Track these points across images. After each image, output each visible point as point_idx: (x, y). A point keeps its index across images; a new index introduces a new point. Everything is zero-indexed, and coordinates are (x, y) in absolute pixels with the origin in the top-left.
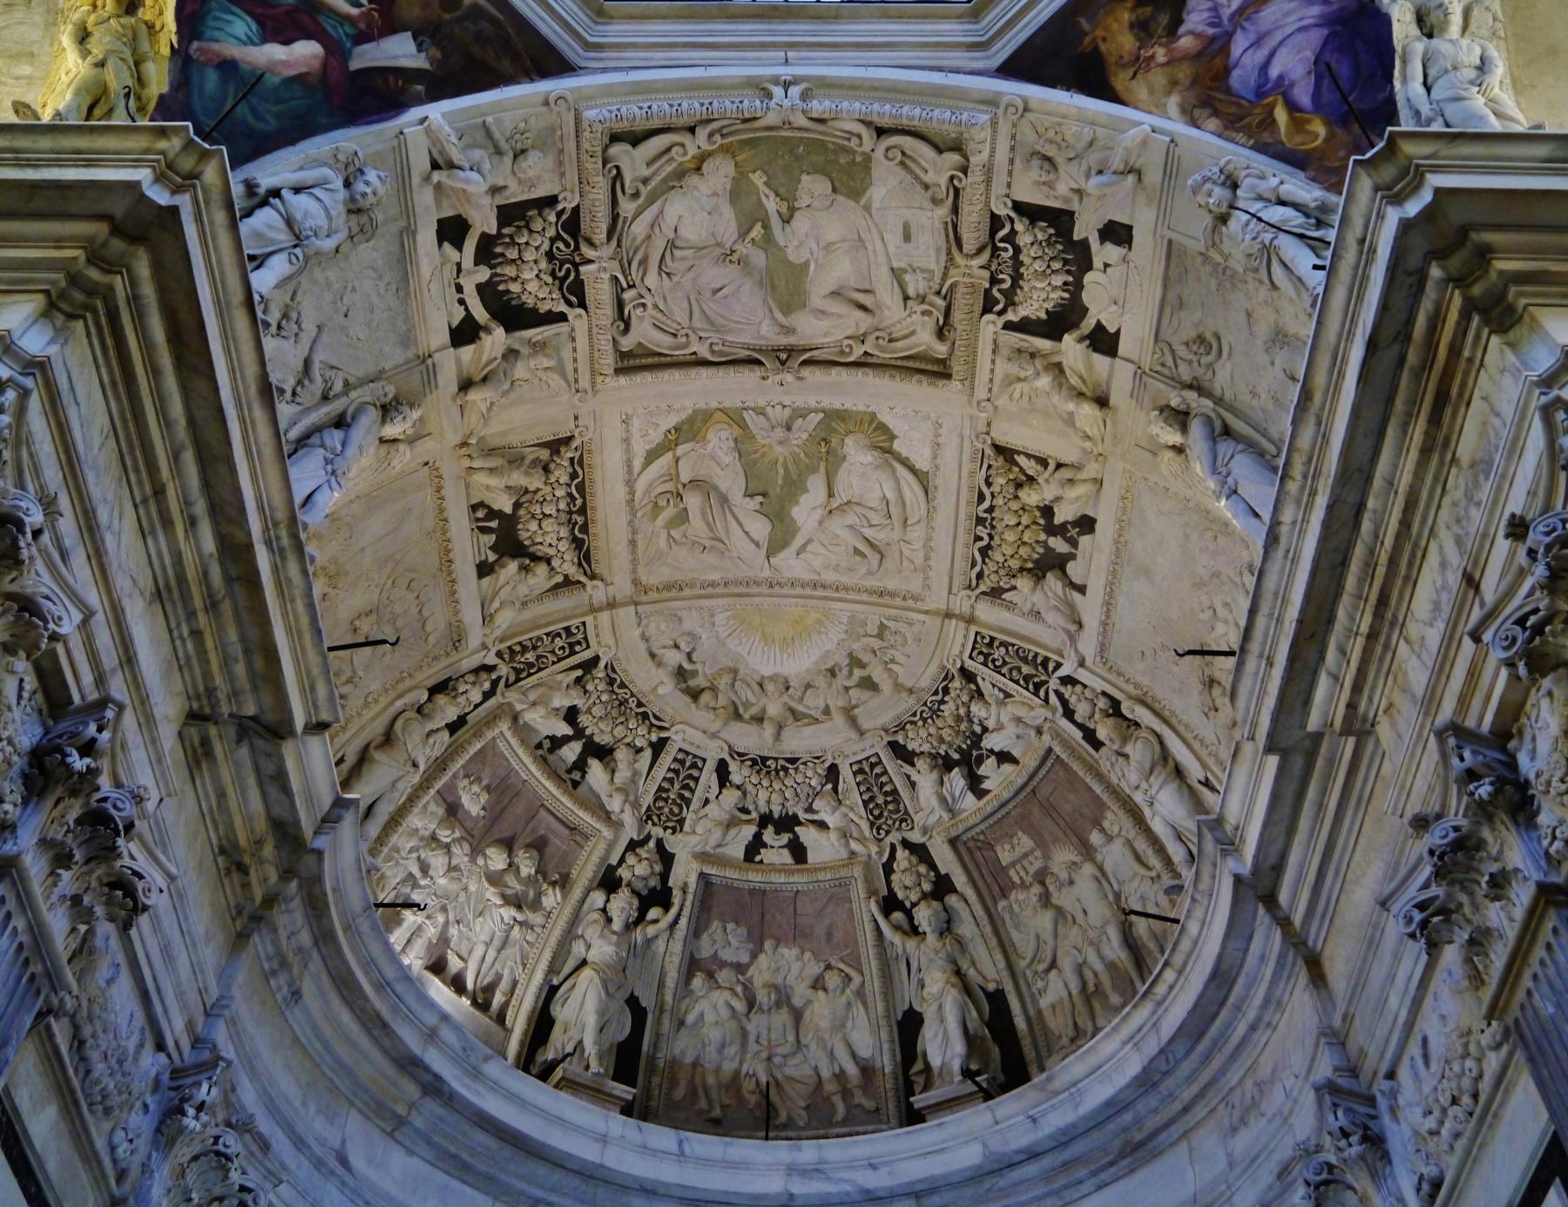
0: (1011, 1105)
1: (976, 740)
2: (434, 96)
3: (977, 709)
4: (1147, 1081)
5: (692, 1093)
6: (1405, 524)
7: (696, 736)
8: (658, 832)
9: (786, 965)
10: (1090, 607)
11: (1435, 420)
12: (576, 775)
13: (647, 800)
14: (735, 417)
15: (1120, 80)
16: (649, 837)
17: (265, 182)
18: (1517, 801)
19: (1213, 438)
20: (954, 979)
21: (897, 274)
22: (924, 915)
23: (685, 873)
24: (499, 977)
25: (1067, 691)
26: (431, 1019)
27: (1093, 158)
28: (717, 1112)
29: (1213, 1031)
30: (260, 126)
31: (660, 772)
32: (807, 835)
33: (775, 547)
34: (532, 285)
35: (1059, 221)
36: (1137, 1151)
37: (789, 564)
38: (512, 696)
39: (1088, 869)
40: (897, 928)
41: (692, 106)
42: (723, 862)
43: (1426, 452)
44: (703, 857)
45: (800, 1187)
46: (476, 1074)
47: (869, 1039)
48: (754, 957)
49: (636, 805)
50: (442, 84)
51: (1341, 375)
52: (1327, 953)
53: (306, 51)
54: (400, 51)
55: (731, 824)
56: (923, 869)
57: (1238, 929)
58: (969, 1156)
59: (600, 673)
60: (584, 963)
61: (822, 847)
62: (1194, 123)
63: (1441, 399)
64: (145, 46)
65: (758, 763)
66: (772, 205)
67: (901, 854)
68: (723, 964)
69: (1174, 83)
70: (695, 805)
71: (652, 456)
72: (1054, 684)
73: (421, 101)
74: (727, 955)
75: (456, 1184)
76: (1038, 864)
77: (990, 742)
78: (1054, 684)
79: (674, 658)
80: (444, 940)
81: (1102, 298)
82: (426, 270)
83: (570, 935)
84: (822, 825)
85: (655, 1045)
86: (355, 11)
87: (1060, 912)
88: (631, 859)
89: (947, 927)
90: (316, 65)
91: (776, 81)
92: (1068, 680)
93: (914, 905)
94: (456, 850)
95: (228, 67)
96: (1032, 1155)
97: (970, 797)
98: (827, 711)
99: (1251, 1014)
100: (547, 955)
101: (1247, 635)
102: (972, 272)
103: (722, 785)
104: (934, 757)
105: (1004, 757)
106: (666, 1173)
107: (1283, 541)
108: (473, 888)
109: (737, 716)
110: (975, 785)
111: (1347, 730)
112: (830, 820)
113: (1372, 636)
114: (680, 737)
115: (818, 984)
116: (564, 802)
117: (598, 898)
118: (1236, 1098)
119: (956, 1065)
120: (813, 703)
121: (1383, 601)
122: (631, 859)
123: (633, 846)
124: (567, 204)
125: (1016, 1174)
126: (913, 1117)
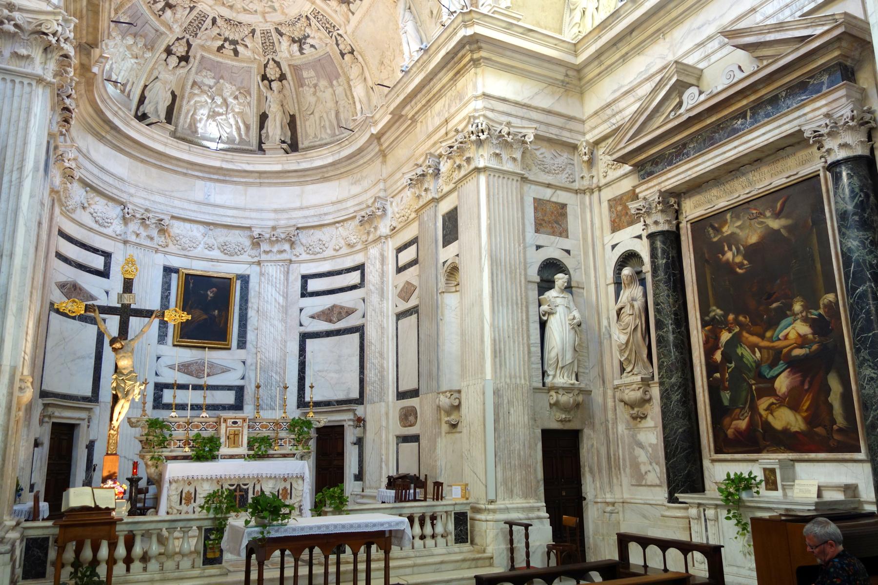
0: (293, 156)
1: (306, 37)
3: (308, 30)
4: (332, 164)
6: (440, 90)
7: (208, 8)
8: (187, 36)
10: (354, 20)
11: (456, 75)
12: (161, 13)
13: (186, 25)
16: (183, 38)
18: (437, 173)
20: (281, 108)
22: (275, 85)
23: (196, 53)
24: (128, 81)
25: (339, 38)
26: (116, 109)
29: (354, 159)
32: (240, 49)
39: (330, 90)
40: (265, 86)
43: (451, 80)
44: (202, 47)
46: (128, 124)
49: (181, 26)
51: (439, 52)
52: (389, 156)
55: (213, 39)
56: (278, 69)
57: (369, 142)
58: (278, 168)
60: (157, 78)
63: (458, 72)
65: (228, 21)
67: (271, 62)
68: (205, 85)
70: (203, 29)
72: (335, 34)
75: (118, 154)
76: (315, 82)
77: (308, 40)
78: (335, 34)
80: (111, 69)
83: (153, 69)
84: (246, 46)
87: (318, 97)
88: (177, 44)
92: (339, 35)
93: (273, 81)
94: (117, 39)
96: (296, 171)
97: (298, 53)
98: (256, 11)
99: (365, 160)
100: (145, 76)
101: (395, 86)
103: (213, 24)
104: (290, 37)
105: (312, 46)
107: (411, 74)
108: (121, 50)
110: (301, 50)
111: (411, 119)
112: (249, 45)
113: (424, 106)
116: (156, 23)
117: (164, 56)
118: (355, 176)
119: (278, 138)
121: (429, 101)
122: (177, 44)
123: (178, 39)
125: (290, 174)
126: (261, 149)
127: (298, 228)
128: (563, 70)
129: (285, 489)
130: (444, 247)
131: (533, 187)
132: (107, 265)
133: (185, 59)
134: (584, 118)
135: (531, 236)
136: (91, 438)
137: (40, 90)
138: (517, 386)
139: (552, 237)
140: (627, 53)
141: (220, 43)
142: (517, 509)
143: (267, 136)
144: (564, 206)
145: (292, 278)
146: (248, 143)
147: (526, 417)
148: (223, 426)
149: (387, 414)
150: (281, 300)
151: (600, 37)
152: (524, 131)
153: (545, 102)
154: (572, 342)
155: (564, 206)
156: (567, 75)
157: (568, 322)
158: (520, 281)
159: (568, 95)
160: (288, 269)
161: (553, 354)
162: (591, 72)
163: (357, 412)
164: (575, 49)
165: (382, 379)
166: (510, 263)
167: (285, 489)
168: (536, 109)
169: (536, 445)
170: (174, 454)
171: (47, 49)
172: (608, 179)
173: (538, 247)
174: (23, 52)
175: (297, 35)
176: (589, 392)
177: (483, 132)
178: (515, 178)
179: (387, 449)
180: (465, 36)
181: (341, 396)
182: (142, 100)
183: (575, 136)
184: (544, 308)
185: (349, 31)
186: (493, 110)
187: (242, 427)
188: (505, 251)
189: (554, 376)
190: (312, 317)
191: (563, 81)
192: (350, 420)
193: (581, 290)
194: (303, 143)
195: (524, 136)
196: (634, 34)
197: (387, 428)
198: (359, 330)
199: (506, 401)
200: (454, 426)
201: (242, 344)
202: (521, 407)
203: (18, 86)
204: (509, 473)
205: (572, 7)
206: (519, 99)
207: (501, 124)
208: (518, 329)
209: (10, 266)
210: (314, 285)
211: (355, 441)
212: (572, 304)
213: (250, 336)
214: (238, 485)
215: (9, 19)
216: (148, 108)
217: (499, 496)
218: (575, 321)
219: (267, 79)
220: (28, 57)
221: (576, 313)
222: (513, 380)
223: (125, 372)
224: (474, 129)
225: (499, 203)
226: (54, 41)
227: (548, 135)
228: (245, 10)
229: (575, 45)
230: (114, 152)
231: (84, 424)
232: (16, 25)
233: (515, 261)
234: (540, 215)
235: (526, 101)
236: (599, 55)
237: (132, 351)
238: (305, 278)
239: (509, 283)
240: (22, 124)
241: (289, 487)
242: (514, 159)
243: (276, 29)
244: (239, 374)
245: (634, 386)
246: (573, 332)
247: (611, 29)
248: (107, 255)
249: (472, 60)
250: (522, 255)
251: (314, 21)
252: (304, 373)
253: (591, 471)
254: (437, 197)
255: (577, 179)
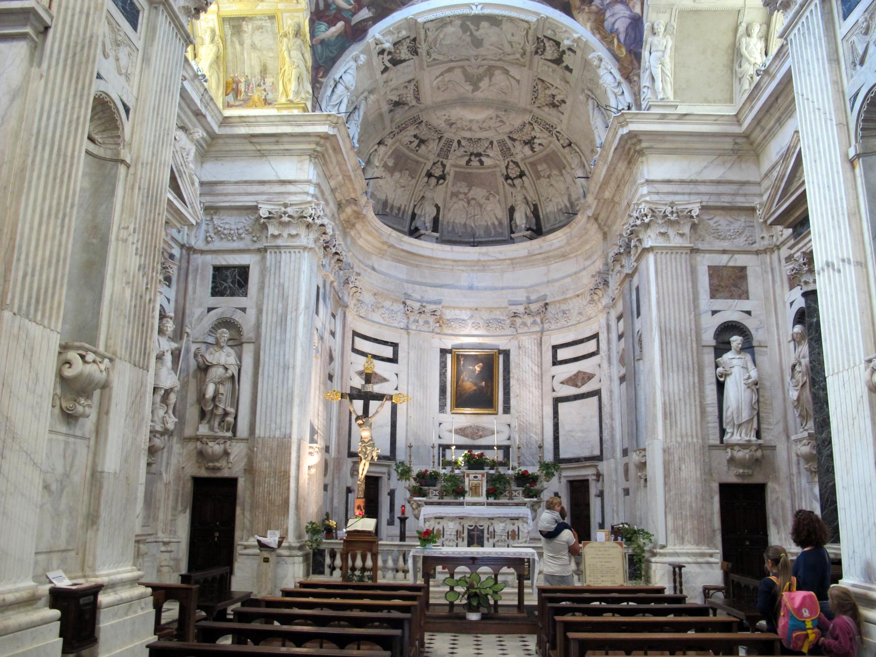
0: (534, 242)
2: (374, 23)
5: (453, 228)
8: (441, 160)
9: (478, 193)
10: (565, 118)
14: (463, 67)
15: (575, 13)
17: (337, 77)
19: (594, 109)
21: (510, 43)
27: (567, 35)
28: (460, 234)
30: (331, 55)
31: (441, 144)
32: (483, 159)
33: (473, 91)
34: (404, 53)
35: (558, 44)
36: (564, 256)
37: (478, 94)
38: (399, 137)
40: (509, 185)
41: (448, 13)
42: (460, 167)
45: (482, 258)
47: (501, 214)
48: (469, 190)
50: (376, 19)
53: (340, 24)
54: (365, 14)
55: (463, 156)
56: (517, 169)
58: (524, 253)
59: (423, 124)
60: (423, 197)
61: (487, 161)
62: (593, 34)
64: (304, 49)
65: (470, 140)
66: (472, 27)
67: (511, 164)
69: (589, 19)
71: (437, 77)
72: (554, 132)
73: (371, 26)
74: (462, 190)
77: (536, 141)
78: (554, 132)
79: (445, 117)
81: (568, 59)
82: (375, 64)
84: (488, 156)
85: (443, 217)
86: (351, 7)
89: (523, 187)
90: (343, 28)
91: (473, 4)
95: (322, 42)
97: (531, 152)
102: (530, 48)
105: (540, 144)
106: (449, 256)
109: (463, 129)
110: (532, 149)
112: (491, 155)
114: (446, 135)
115: (488, 199)
117: (426, 179)
119: (523, 226)
120: (485, 125)
123: (434, 164)
124: (412, 37)
127: (547, 304)
128: (730, 140)
129: (513, 531)
130: (638, 317)
131: (707, 256)
132: (396, 353)
133: (443, 177)
134: (758, 180)
135: (705, 302)
136: (392, 487)
137: (306, 254)
138: (688, 445)
139: (730, 301)
140: (780, 118)
141: (467, 158)
142: (688, 554)
143: (516, 226)
144: (743, 269)
145: (544, 349)
146: (501, 234)
147: (698, 473)
148: (467, 479)
149: (616, 470)
150: (536, 369)
151: (753, 107)
152: (690, 207)
153: (715, 173)
154: (748, 399)
155: (743, 269)
156: (736, 143)
157: (743, 382)
158: (692, 347)
159: (741, 161)
160: (541, 341)
161: (729, 413)
162: (758, 136)
163: (599, 468)
164: (737, 119)
165: (613, 437)
166: (681, 332)
167: (513, 531)
168: (704, 182)
169: (712, 498)
170: (431, 500)
171: (309, 226)
172: (784, 237)
173: (714, 312)
174: (294, 232)
175: (525, 138)
176: (774, 448)
177: (646, 216)
178: (684, 251)
179: (617, 500)
180: (622, 136)
181: (587, 454)
182: (414, 216)
183: (750, 199)
184: (720, 370)
185: (564, 128)
186: (658, 193)
187: (482, 480)
188: (675, 320)
189: (733, 434)
190: (562, 383)
191: (733, 150)
192: (593, 475)
193: (765, 349)
194: (545, 227)
195: (690, 211)
196: (779, 101)
197: (616, 482)
198: (597, 393)
199: (676, 458)
200: (646, 480)
201: (507, 410)
202: (693, 464)
203: (293, 254)
204: (680, 522)
205: (740, 76)
206: (686, 177)
207: (666, 204)
208: (690, 392)
209: (294, 374)
210: (562, 354)
211: (598, 492)
212: (750, 364)
213: (513, 402)
214: (476, 526)
215: (285, 213)
216: (418, 223)
217: (670, 542)
218: (750, 381)
219: (510, 178)
220: (297, 234)
221: (754, 373)
222: (685, 439)
223: (366, 440)
224: (637, 215)
225: (667, 278)
226: (310, 220)
227: (719, 204)
228: (481, 128)
229: (736, 116)
230: (394, 264)
231: (385, 477)
232: (290, 216)
233: (685, 329)
234: (715, 281)
235: (694, 178)
236: (758, 121)
237: (370, 426)
238: (555, 348)
239: (679, 351)
240: (296, 280)
241: (516, 529)
242: (682, 235)
243: (509, 137)
244: (506, 436)
245: (805, 441)
246: (749, 391)
247: (759, 99)
248: (395, 346)
249: (635, 151)
250: (693, 323)
251: (536, 126)
252: (558, 433)
253: (776, 523)
254: (630, 272)
255: (758, 239)
